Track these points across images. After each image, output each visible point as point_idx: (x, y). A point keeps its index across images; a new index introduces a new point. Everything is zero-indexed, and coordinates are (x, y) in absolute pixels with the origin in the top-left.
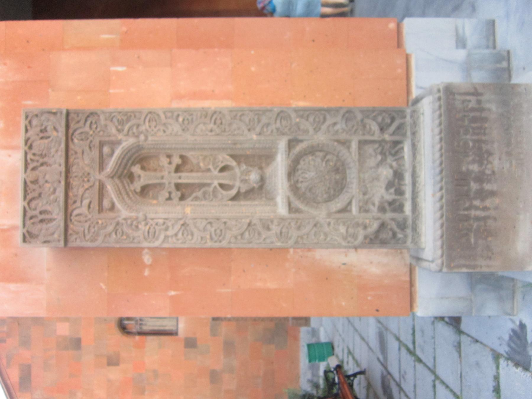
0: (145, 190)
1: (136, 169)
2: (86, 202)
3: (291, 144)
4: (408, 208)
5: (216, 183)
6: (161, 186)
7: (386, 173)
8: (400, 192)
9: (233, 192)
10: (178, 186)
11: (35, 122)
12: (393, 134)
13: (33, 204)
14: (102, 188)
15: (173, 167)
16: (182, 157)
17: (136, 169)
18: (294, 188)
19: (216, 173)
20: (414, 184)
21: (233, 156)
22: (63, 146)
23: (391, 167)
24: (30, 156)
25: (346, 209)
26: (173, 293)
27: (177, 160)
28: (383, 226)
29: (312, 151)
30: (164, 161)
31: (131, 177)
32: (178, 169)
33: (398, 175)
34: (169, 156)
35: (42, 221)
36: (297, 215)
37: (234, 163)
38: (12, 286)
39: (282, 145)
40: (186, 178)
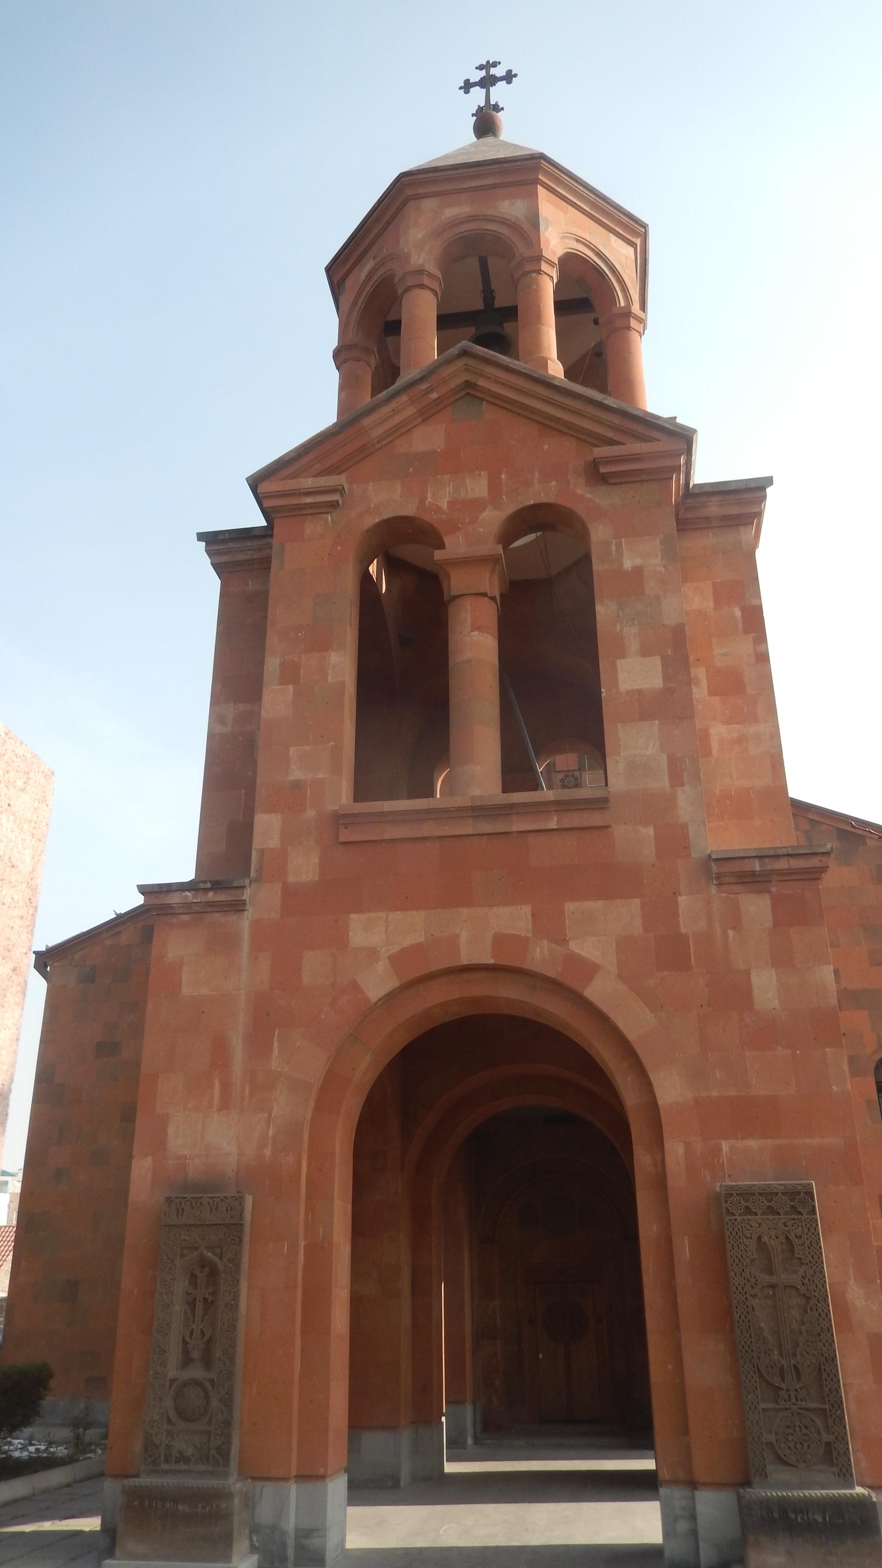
0: (193, 1276)
1: (207, 1270)
2: (187, 1238)
3: (212, 1381)
4: (165, 1466)
5: (194, 1326)
6: (195, 1288)
7: (189, 1452)
8: (177, 1461)
9: (188, 1340)
10: (195, 1299)
11: (237, 1202)
12: (213, 1457)
13: (188, 1204)
14: (197, 1249)
15: (207, 1296)
16: (212, 1302)
17: (207, 1270)
18: (185, 1384)
19: (201, 1327)
20: (180, 1472)
21: (210, 1339)
22: (221, 1222)
23: (192, 1455)
24: (217, 1200)
25: (169, 1421)
26: (136, 1292)
27: (210, 1299)
28: (157, 1447)
29: (207, 1397)
30: (211, 1289)
31: (203, 1266)
32: (205, 1299)
33: (187, 1460)
34: (213, 1293)
35: (178, 1210)
36: (168, 1384)
37: (205, 1339)
38: (150, 1176)
39: (213, 1375)
40: (199, 1306)
